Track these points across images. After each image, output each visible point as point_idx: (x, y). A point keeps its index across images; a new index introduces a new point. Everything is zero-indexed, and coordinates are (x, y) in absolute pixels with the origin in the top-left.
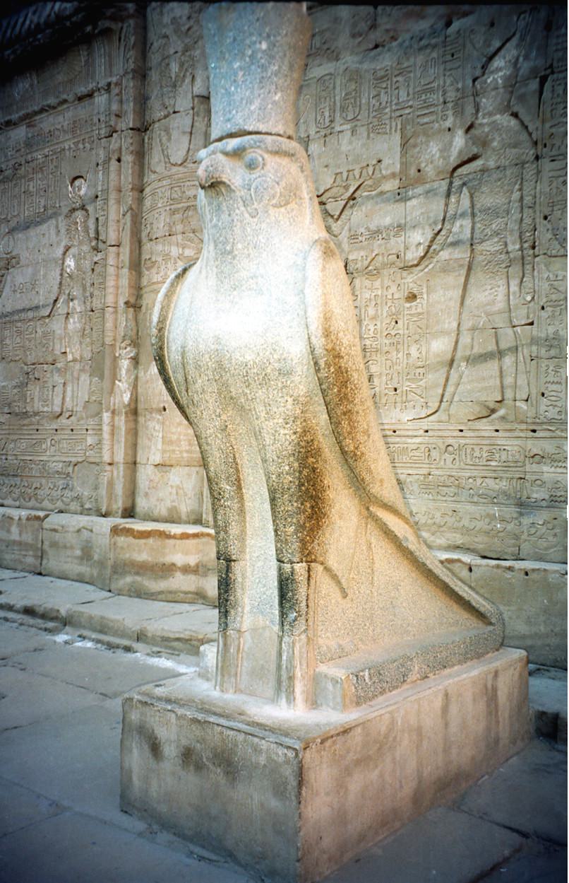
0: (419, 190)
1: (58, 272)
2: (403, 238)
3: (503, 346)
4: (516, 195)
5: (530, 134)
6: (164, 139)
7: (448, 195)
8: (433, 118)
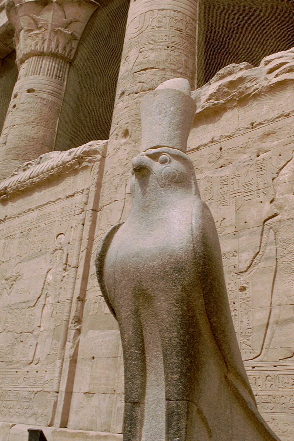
8: (253, 196)
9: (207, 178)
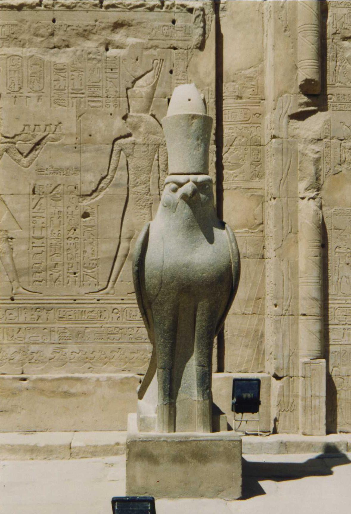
2: (79, 176)
9: (33, 58)
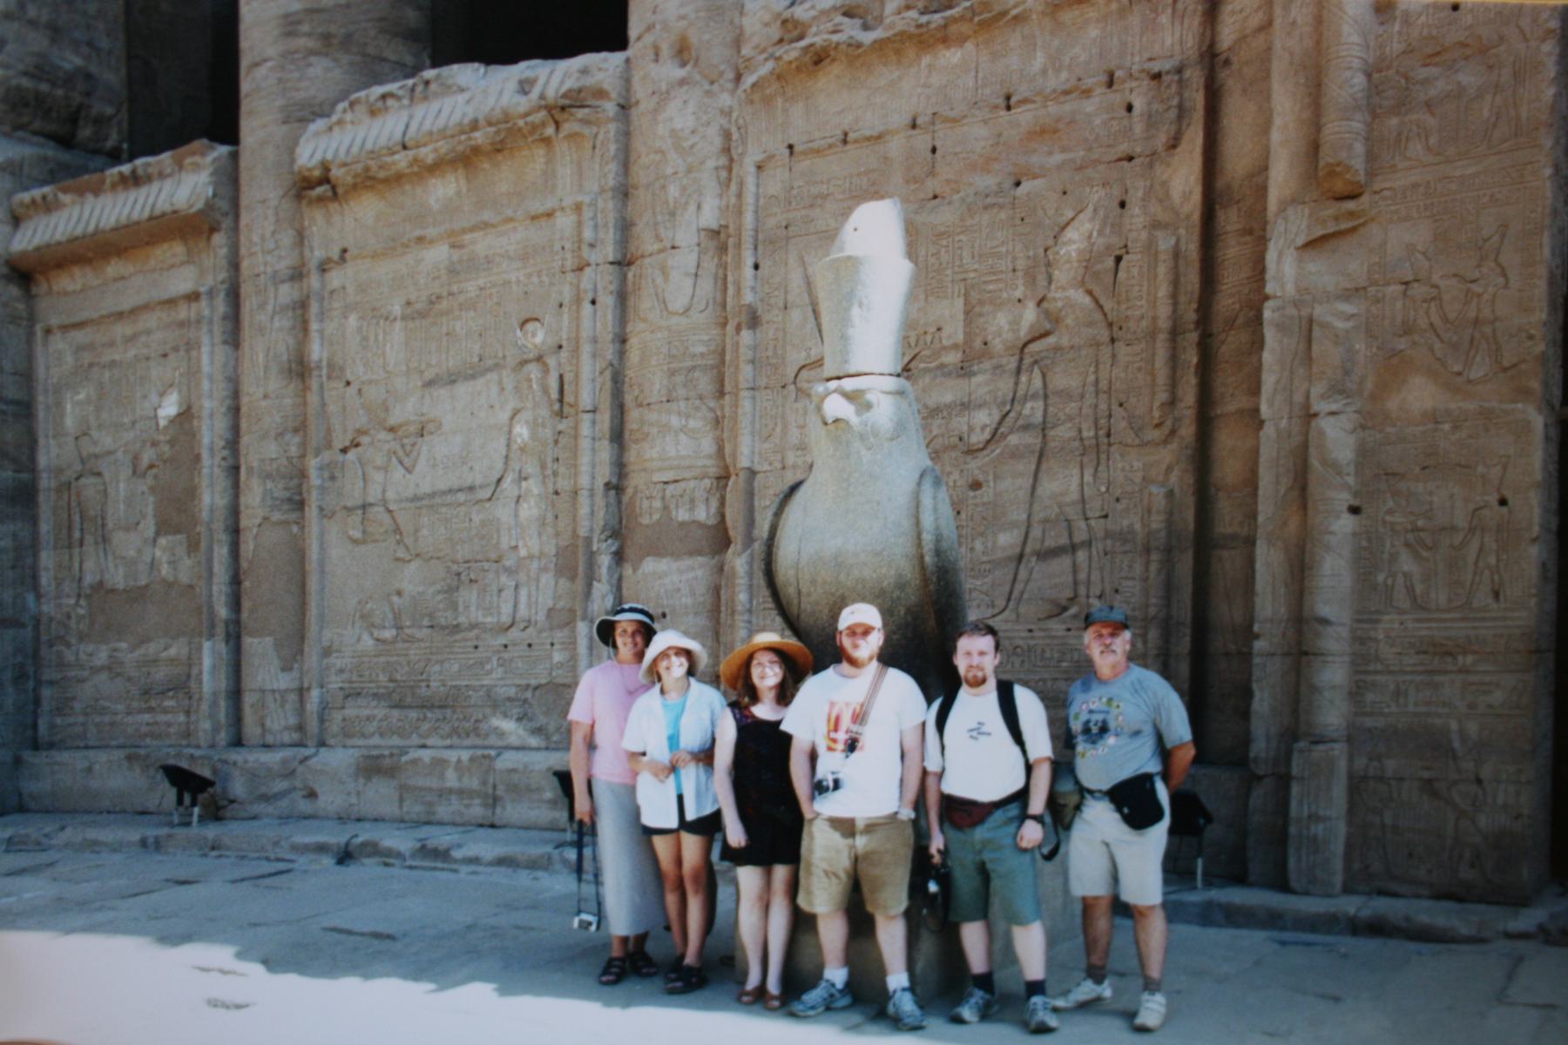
0: (987, 365)
1: (503, 441)
3: (1078, 538)
4: (1092, 378)
5: (1105, 315)
6: (659, 280)
7: (1018, 371)
8: (1001, 286)
